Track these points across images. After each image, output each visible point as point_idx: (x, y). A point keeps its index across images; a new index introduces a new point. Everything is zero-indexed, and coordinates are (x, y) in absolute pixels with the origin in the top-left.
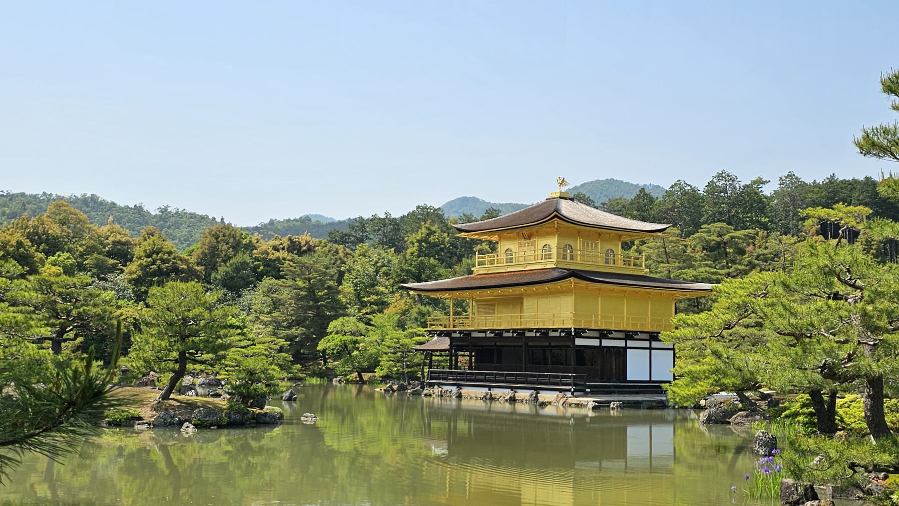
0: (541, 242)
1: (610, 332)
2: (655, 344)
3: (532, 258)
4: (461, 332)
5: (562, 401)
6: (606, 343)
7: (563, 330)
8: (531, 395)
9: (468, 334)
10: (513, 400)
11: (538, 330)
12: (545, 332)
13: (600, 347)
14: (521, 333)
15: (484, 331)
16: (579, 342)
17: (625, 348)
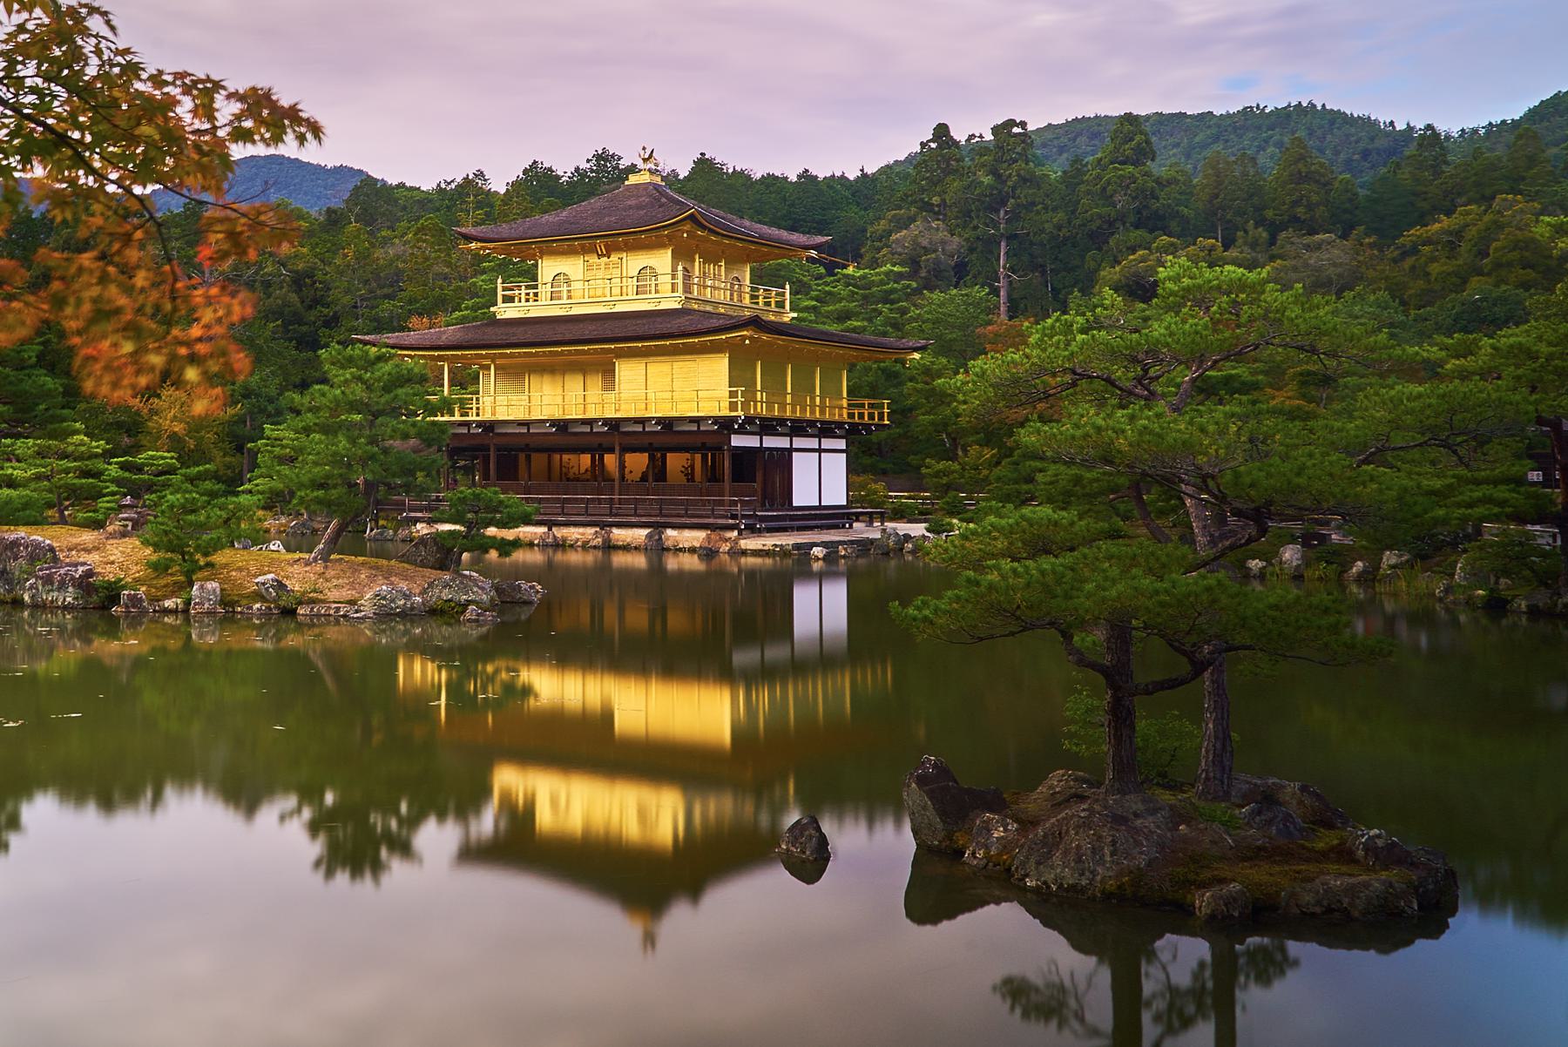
0: (635, 262)
1: (782, 421)
2: (827, 443)
3: (616, 291)
4: (480, 424)
5: (725, 547)
6: (771, 442)
7: (716, 420)
8: (649, 536)
9: (489, 426)
10: (609, 547)
11: (659, 421)
12: (667, 423)
13: (761, 450)
14: (614, 424)
15: (526, 424)
16: (737, 441)
17: (791, 450)
